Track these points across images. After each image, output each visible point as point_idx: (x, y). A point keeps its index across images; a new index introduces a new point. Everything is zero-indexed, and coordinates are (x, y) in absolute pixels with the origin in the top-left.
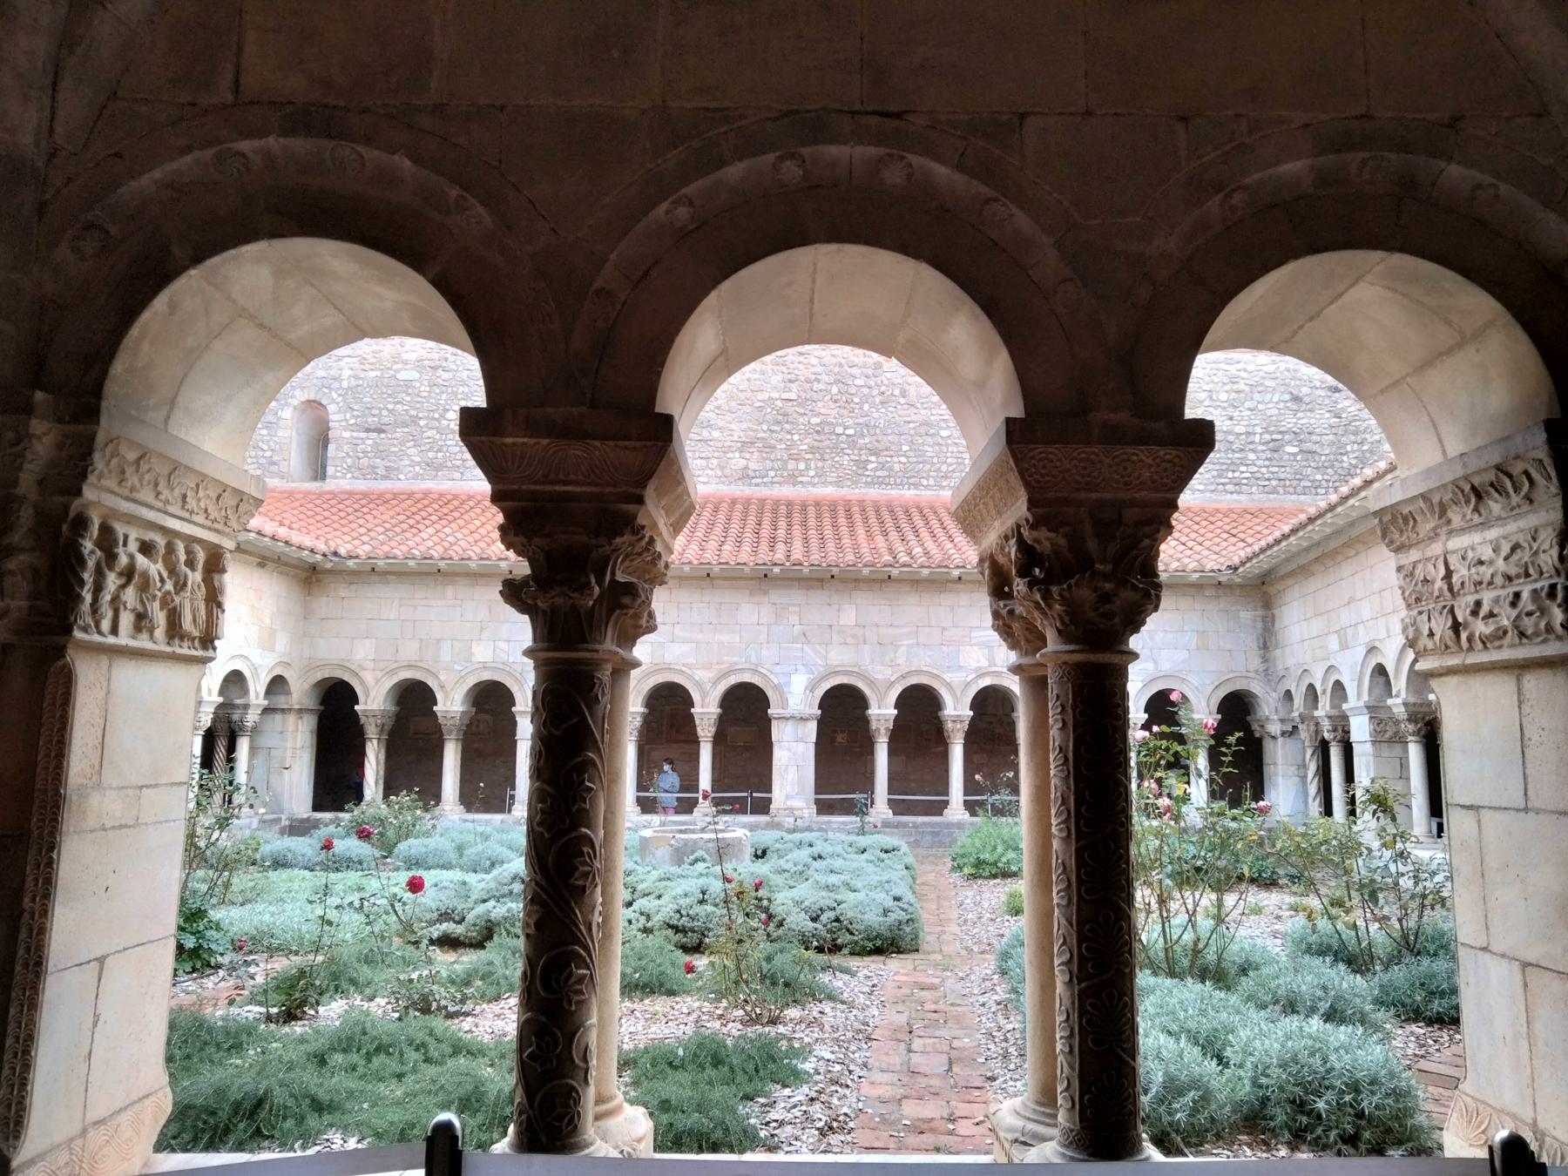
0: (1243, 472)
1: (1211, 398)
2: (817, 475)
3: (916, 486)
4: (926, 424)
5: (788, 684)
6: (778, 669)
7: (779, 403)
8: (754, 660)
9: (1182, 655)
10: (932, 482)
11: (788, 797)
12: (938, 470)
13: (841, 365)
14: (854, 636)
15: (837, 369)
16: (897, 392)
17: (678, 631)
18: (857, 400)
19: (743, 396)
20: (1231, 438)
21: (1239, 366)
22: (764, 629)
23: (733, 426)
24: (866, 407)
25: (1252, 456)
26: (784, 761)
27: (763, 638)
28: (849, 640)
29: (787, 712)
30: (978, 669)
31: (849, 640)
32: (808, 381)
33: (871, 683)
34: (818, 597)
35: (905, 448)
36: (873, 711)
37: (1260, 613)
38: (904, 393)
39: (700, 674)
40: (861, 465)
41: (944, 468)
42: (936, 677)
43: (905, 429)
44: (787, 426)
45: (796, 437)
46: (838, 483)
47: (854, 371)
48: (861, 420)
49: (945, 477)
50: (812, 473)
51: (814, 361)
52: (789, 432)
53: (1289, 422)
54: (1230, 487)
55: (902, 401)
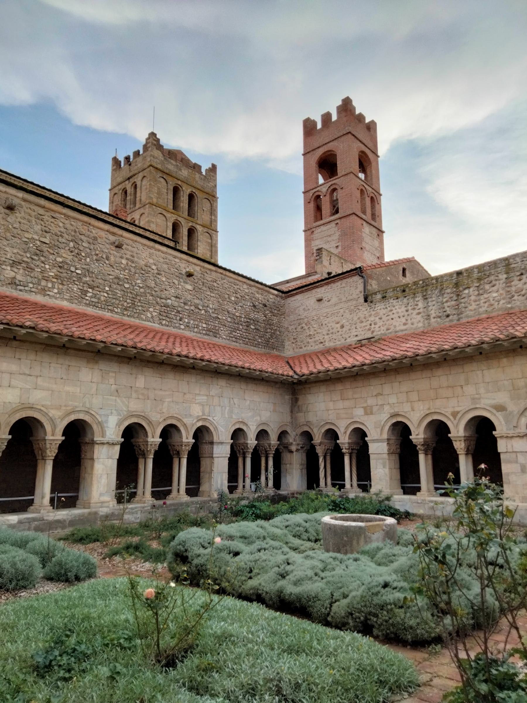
0: (238, 334)
1: (229, 298)
2: (59, 293)
3: (112, 311)
4: (118, 278)
5: (107, 422)
6: (101, 412)
7: (38, 242)
8: (88, 405)
9: (268, 414)
10: (119, 310)
11: (101, 495)
12: (123, 305)
13: (75, 232)
14: (143, 394)
15: (73, 233)
16: (104, 256)
17: (40, 381)
18: (83, 254)
19: (15, 231)
20: (235, 317)
21: (238, 287)
22: (94, 386)
23: (7, 249)
24: (88, 260)
25: (241, 327)
26: (100, 472)
27: (94, 390)
28: (140, 397)
29: (105, 440)
30: (198, 416)
31: (140, 397)
32: (56, 235)
33: (150, 423)
34: (125, 369)
35: (107, 289)
36: (150, 439)
37: (291, 396)
38: (108, 258)
39: (53, 413)
40: (84, 293)
41: (125, 304)
42: (179, 420)
43: (108, 278)
44: (43, 259)
45: (47, 267)
46: (70, 300)
47: (82, 237)
48: (84, 266)
49: (126, 309)
50: (56, 291)
51: (61, 225)
52: (43, 262)
53: (252, 316)
54: (234, 339)
55: (107, 262)
